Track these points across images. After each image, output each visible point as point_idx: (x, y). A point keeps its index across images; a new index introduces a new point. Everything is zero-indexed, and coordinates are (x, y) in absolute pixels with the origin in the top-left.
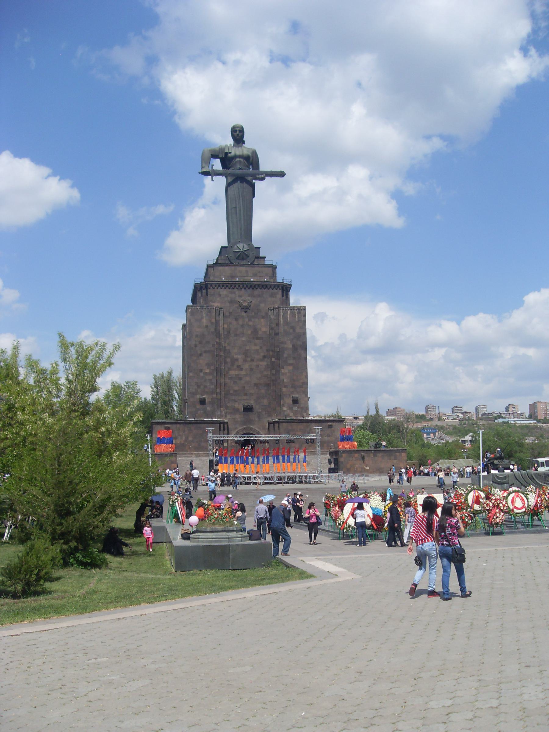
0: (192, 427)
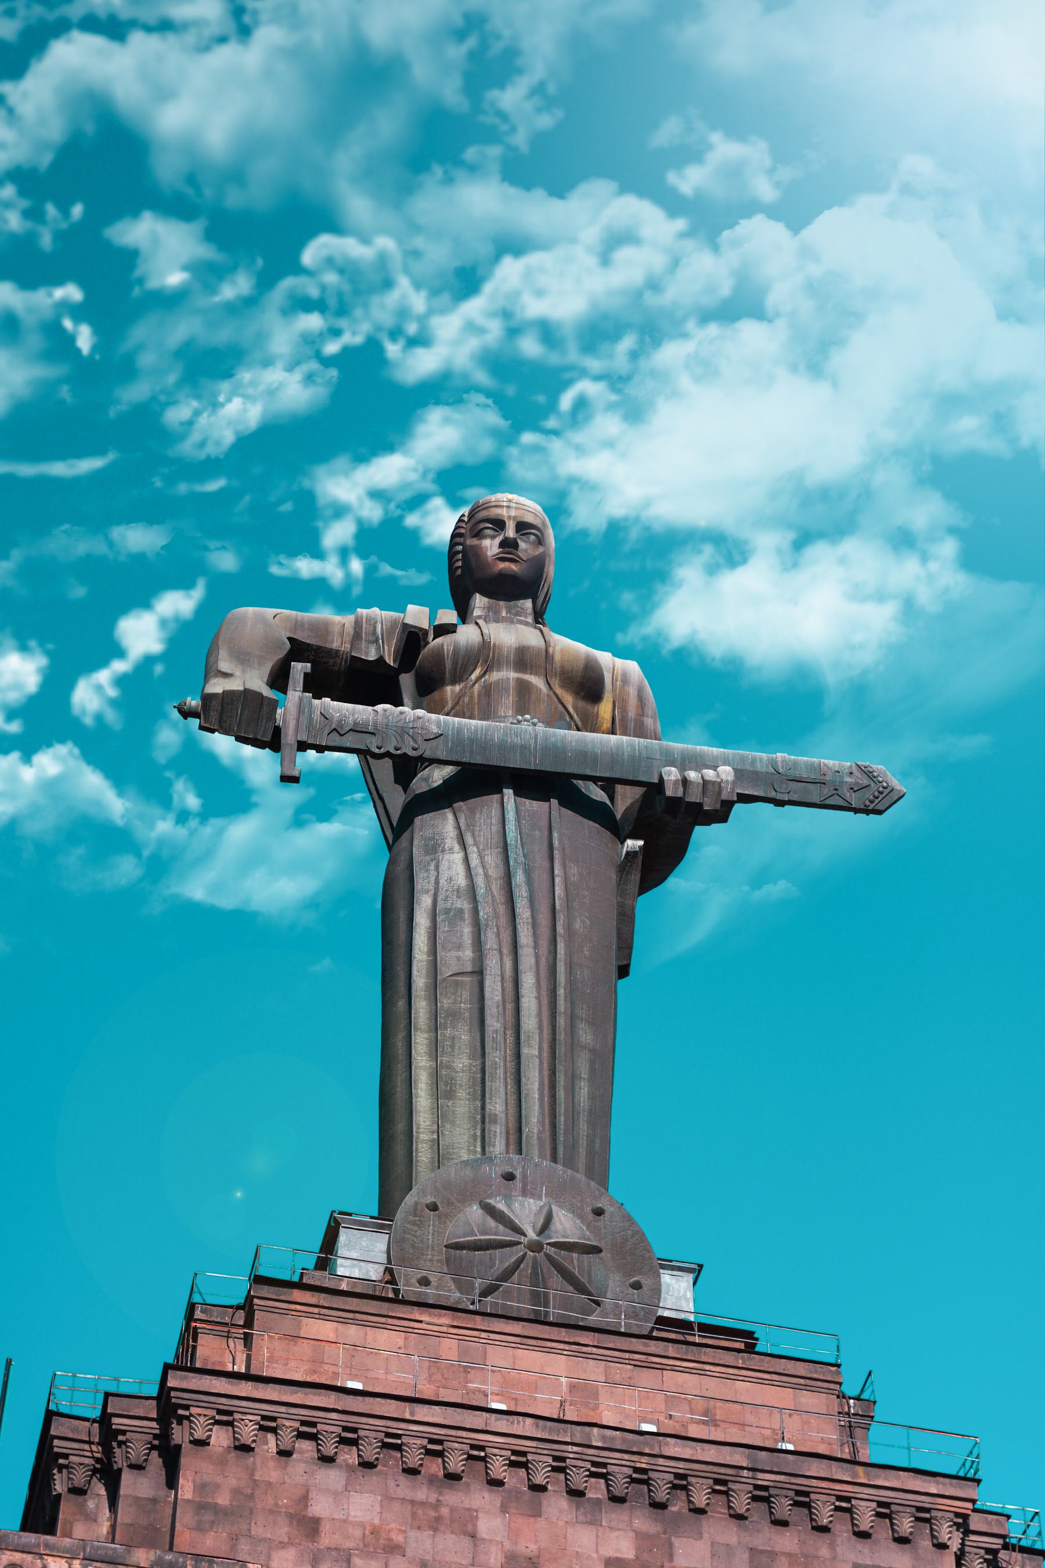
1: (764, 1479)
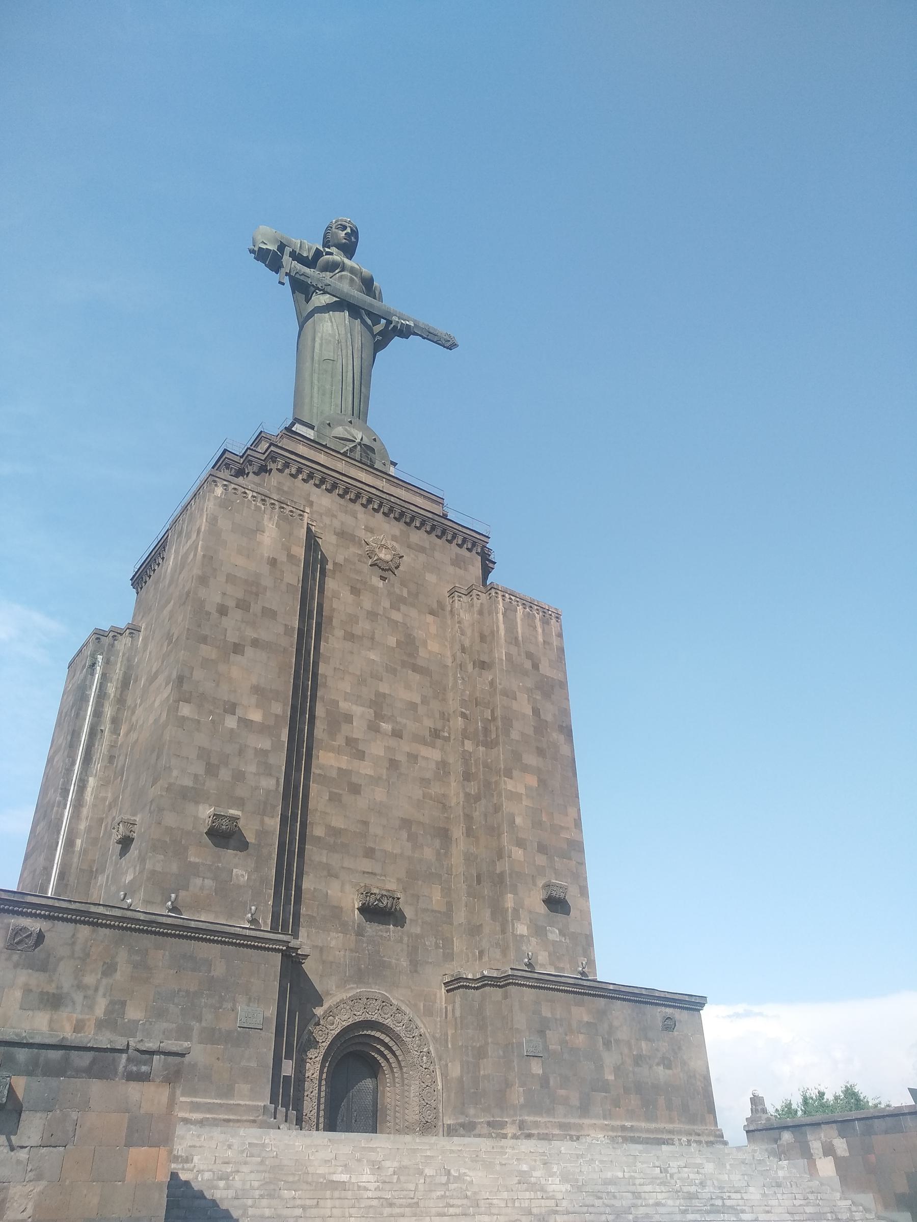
0: (161, 954)
1: (435, 523)
